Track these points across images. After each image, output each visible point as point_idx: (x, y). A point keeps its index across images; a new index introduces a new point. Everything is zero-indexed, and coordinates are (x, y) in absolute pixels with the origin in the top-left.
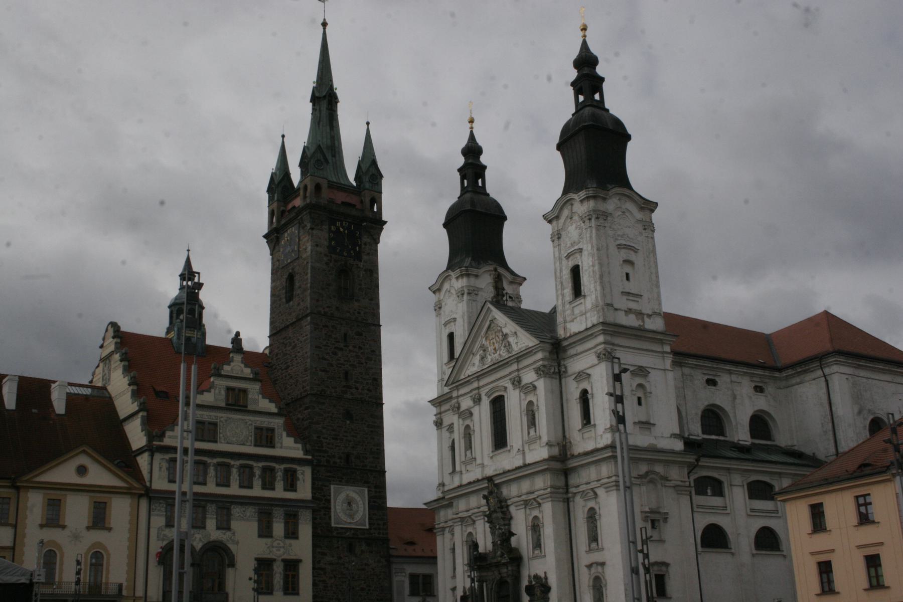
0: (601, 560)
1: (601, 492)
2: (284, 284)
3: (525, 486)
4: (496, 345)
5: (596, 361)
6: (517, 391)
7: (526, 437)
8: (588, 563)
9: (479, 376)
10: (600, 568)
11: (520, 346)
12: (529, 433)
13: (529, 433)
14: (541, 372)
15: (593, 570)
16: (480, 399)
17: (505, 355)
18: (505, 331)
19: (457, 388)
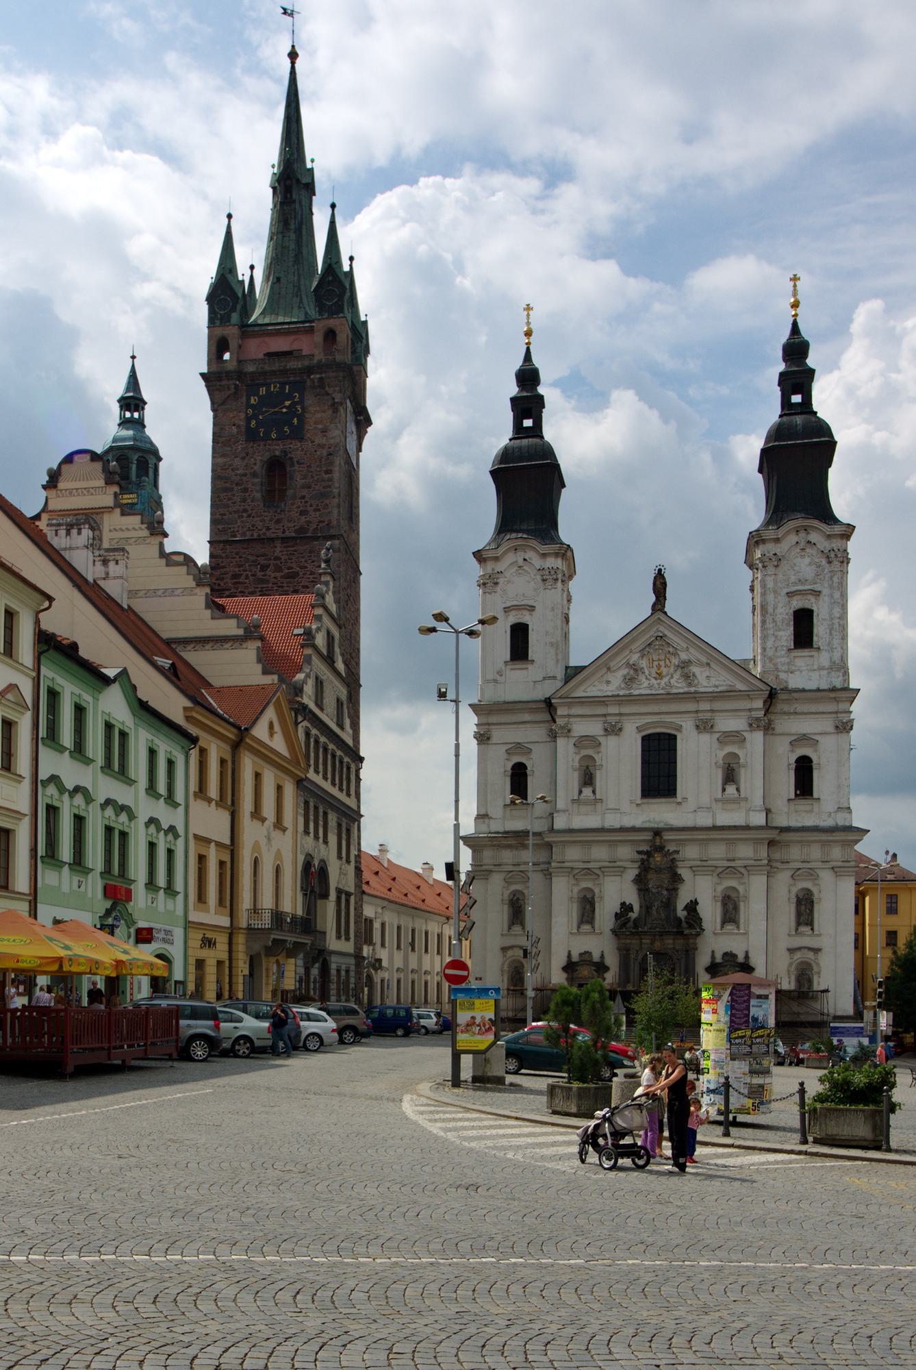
0: (815, 945)
1: (826, 877)
2: (257, 468)
3: (717, 852)
4: (664, 670)
5: (832, 729)
6: (705, 738)
7: (719, 796)
8: (790, 947)
9: (617, 699)
10: (811, 955)
11: (713, 681)
12: (724, 790)
13: (724, 790)
14: (754, 725)
15: (798, 955)
16: (620, 729)
17: (679, 686)
18: (684, 656)
19: (569, 705)
